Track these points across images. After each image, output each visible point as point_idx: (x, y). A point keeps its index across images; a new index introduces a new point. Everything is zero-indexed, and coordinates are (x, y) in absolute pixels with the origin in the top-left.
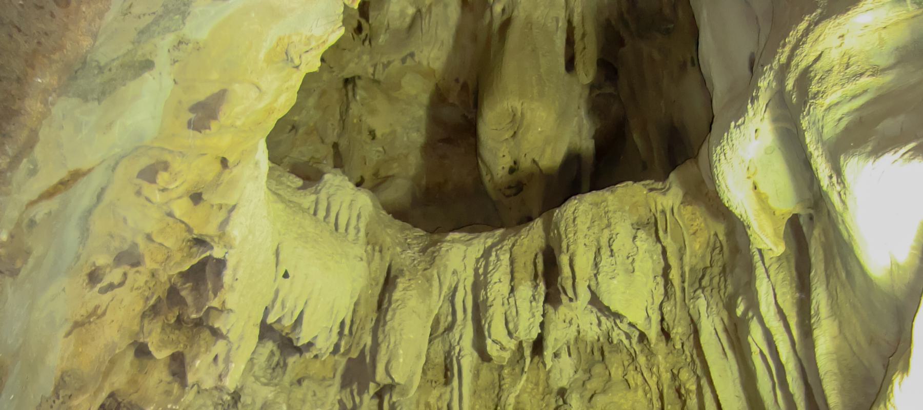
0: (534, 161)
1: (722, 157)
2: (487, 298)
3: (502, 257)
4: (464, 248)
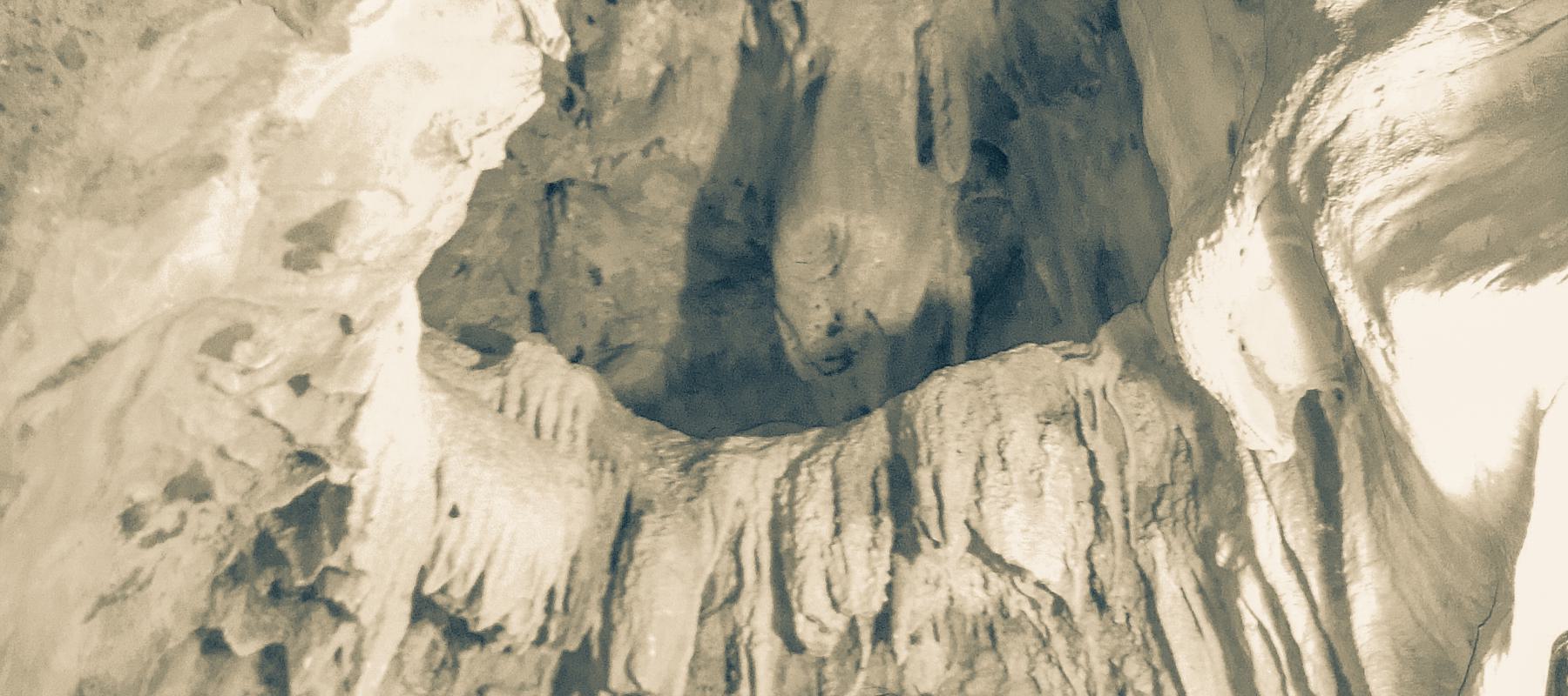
0: (870, 315)
2: (795, 545)
3: (818, 476)
4: (753, 461)
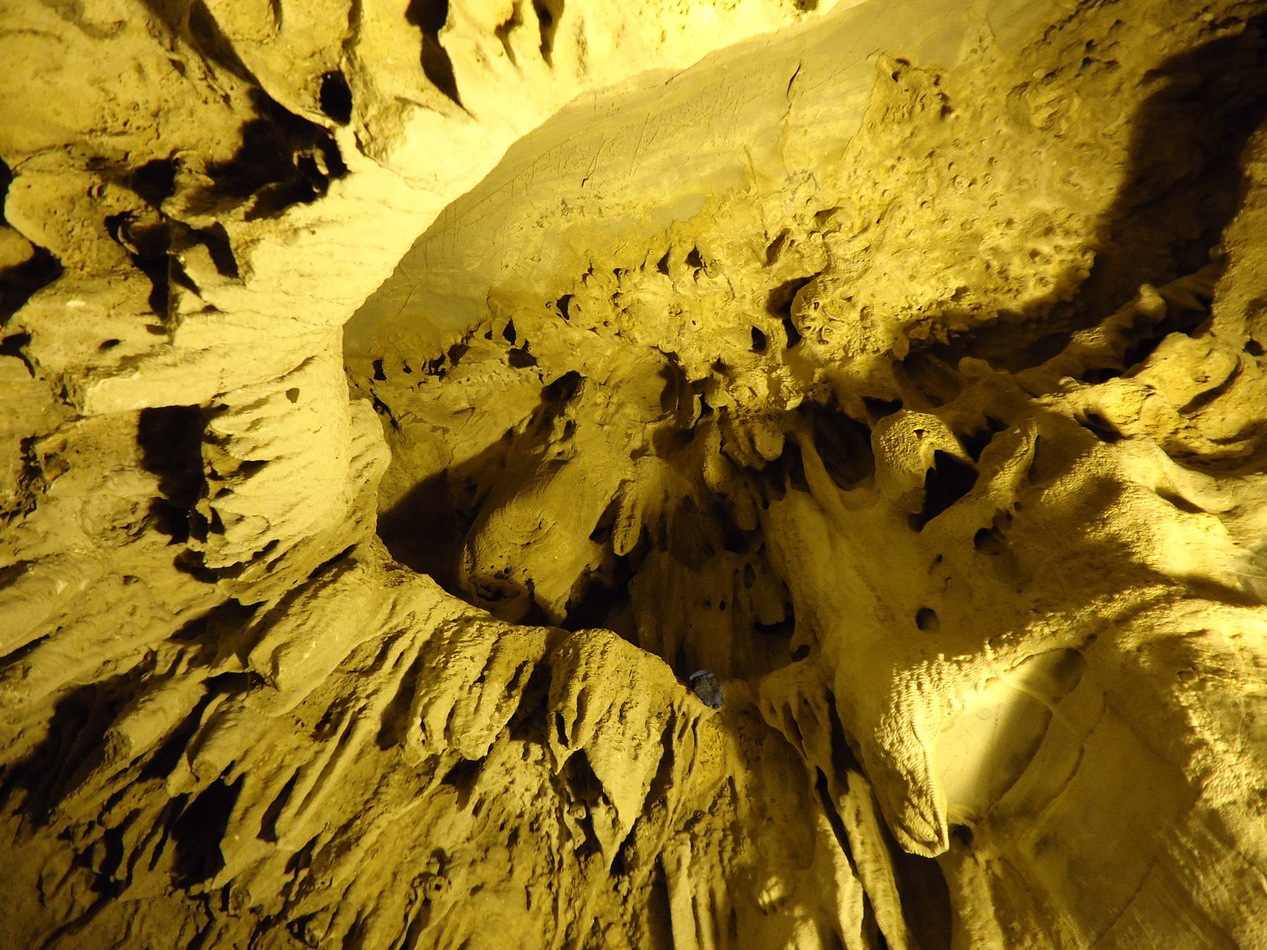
0: (529, 582)
1: (914, 685)
2: (445, 668)
